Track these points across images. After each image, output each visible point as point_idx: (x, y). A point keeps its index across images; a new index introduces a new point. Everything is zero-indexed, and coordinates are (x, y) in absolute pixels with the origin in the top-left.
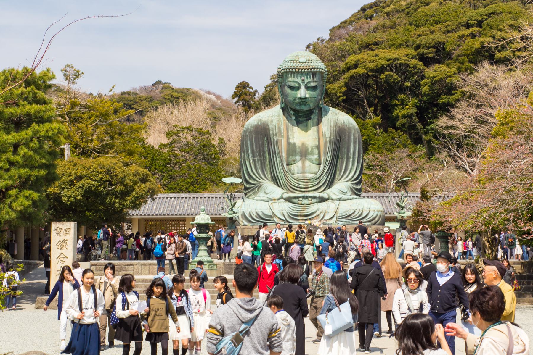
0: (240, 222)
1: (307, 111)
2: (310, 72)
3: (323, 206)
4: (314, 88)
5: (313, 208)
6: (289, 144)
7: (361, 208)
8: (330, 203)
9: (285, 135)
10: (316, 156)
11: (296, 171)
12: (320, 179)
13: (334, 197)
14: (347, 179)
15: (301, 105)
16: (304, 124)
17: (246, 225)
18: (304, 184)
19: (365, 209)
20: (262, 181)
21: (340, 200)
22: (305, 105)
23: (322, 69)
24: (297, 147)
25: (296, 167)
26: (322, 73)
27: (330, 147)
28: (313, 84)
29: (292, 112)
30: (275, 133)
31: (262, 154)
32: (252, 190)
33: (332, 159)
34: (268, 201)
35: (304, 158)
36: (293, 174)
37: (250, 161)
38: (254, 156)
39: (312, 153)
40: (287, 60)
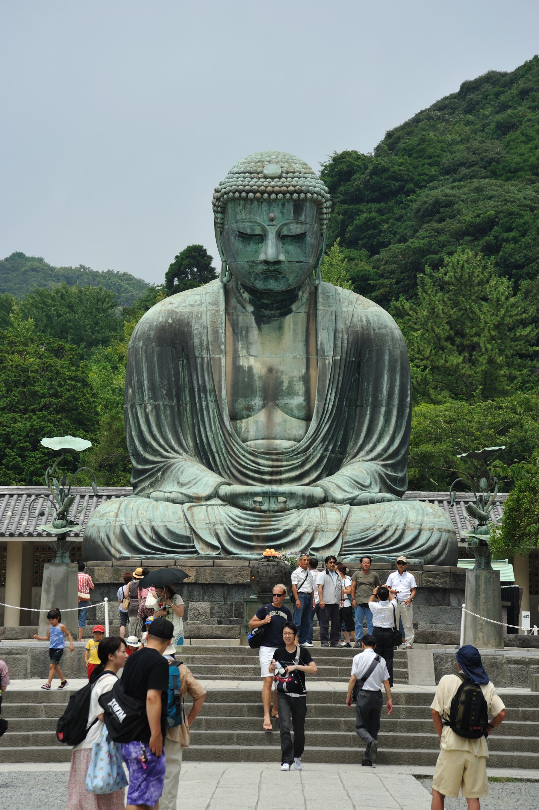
0: (113, 551)
1: (281, 293)
2: (288, 200)
3: (311, 516)
4: (299, 238)
5: (288, 521)
6: (237, 369)
7: (400, 522)
8: (328, 509)
9: (229, 349)
10: (299, 400)
11: (252, 433)
12: (308, 453)
13: (339, 495)
15: (266, 279)
16: (275, 324)
17: (127, 558)
18: (270, 463)
19: (411, 525)
20: (172, 454)
21: (351, 504)
22: (277, 279)
23: (318, 194)
24: (256, 378)
25: (253, 425)
26: (318, 204)
27: (332, 379)
28: (296, 229)
29: (246, 295)
30: (205, 343)
31: (176, 391)
32: (150, 476)
33: (339, 407)
34: (182, 503)
36: (245, 441)
37: (145, 408)
38: (154, 397)
39: (291, 393)
40: (236, 170)
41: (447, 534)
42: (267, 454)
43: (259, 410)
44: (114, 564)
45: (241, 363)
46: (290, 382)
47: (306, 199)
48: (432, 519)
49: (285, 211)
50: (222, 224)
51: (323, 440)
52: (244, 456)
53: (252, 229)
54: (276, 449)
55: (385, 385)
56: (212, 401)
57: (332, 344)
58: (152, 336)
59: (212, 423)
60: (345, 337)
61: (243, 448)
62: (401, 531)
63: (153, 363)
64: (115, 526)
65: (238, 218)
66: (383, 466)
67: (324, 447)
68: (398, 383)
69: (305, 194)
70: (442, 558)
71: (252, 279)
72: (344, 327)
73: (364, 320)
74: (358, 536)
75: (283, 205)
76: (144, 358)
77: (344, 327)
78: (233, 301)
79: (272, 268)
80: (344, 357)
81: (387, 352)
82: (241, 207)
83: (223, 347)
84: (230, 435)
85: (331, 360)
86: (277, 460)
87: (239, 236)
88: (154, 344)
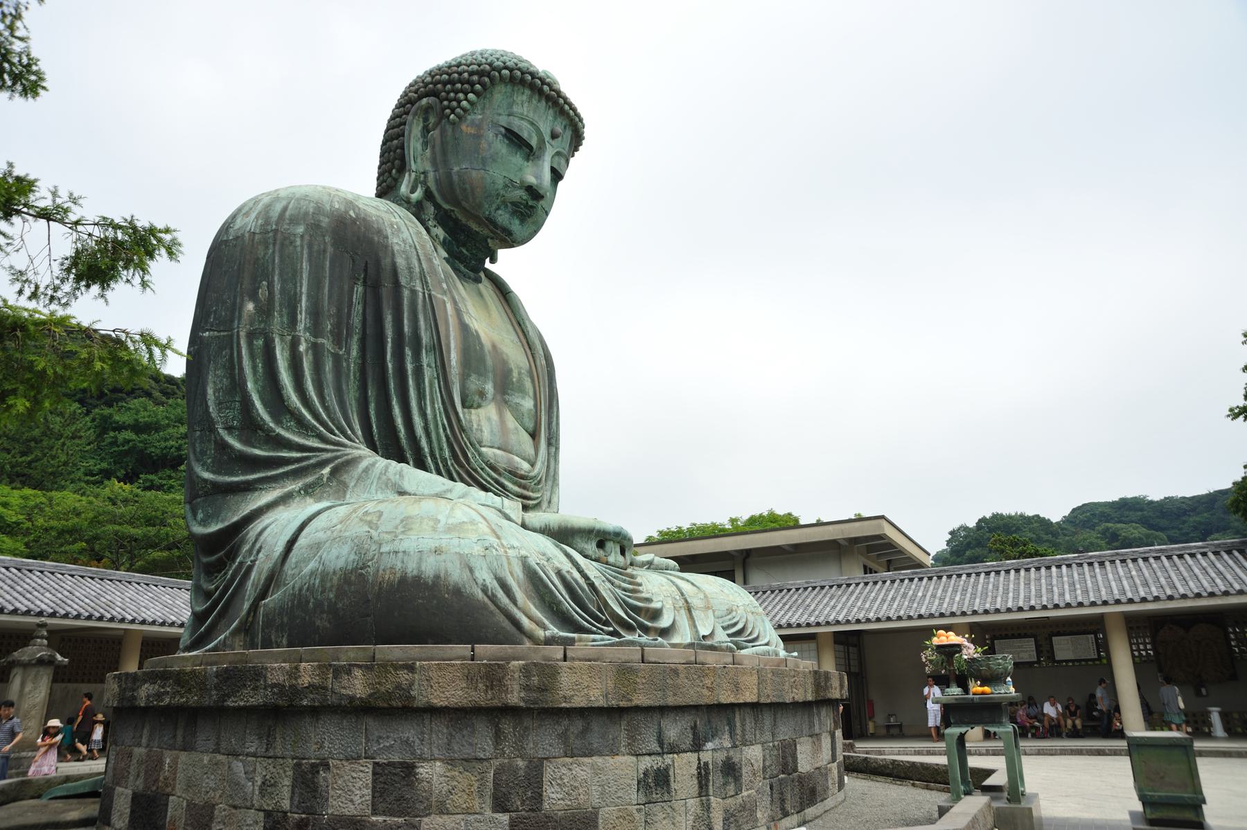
10: (528, 404)
11: (486, 435)
15: (514, 213)
22: (522, 221)
30: (417, 270)
32: (296, 474)
35: (498, 397)
38: (316, 329)
39: (521, 390)
42: (510, 472)
44: (569, 654)
46: (520, 373)
50: (465, 110)
53: (530, 135)
56: (429, 365)
58: (323, 225)
59: (428, 402)
61: (480, 454)
63: (323, 268)
64: (508, 558)
65: (515, 109)
71: (494, 206)
76: (305, 256)
79: (530, 203)
82: (525, 98)
83: (445, 286)
84: (462, 429)
87: (505, 136)
88: (327, 239)
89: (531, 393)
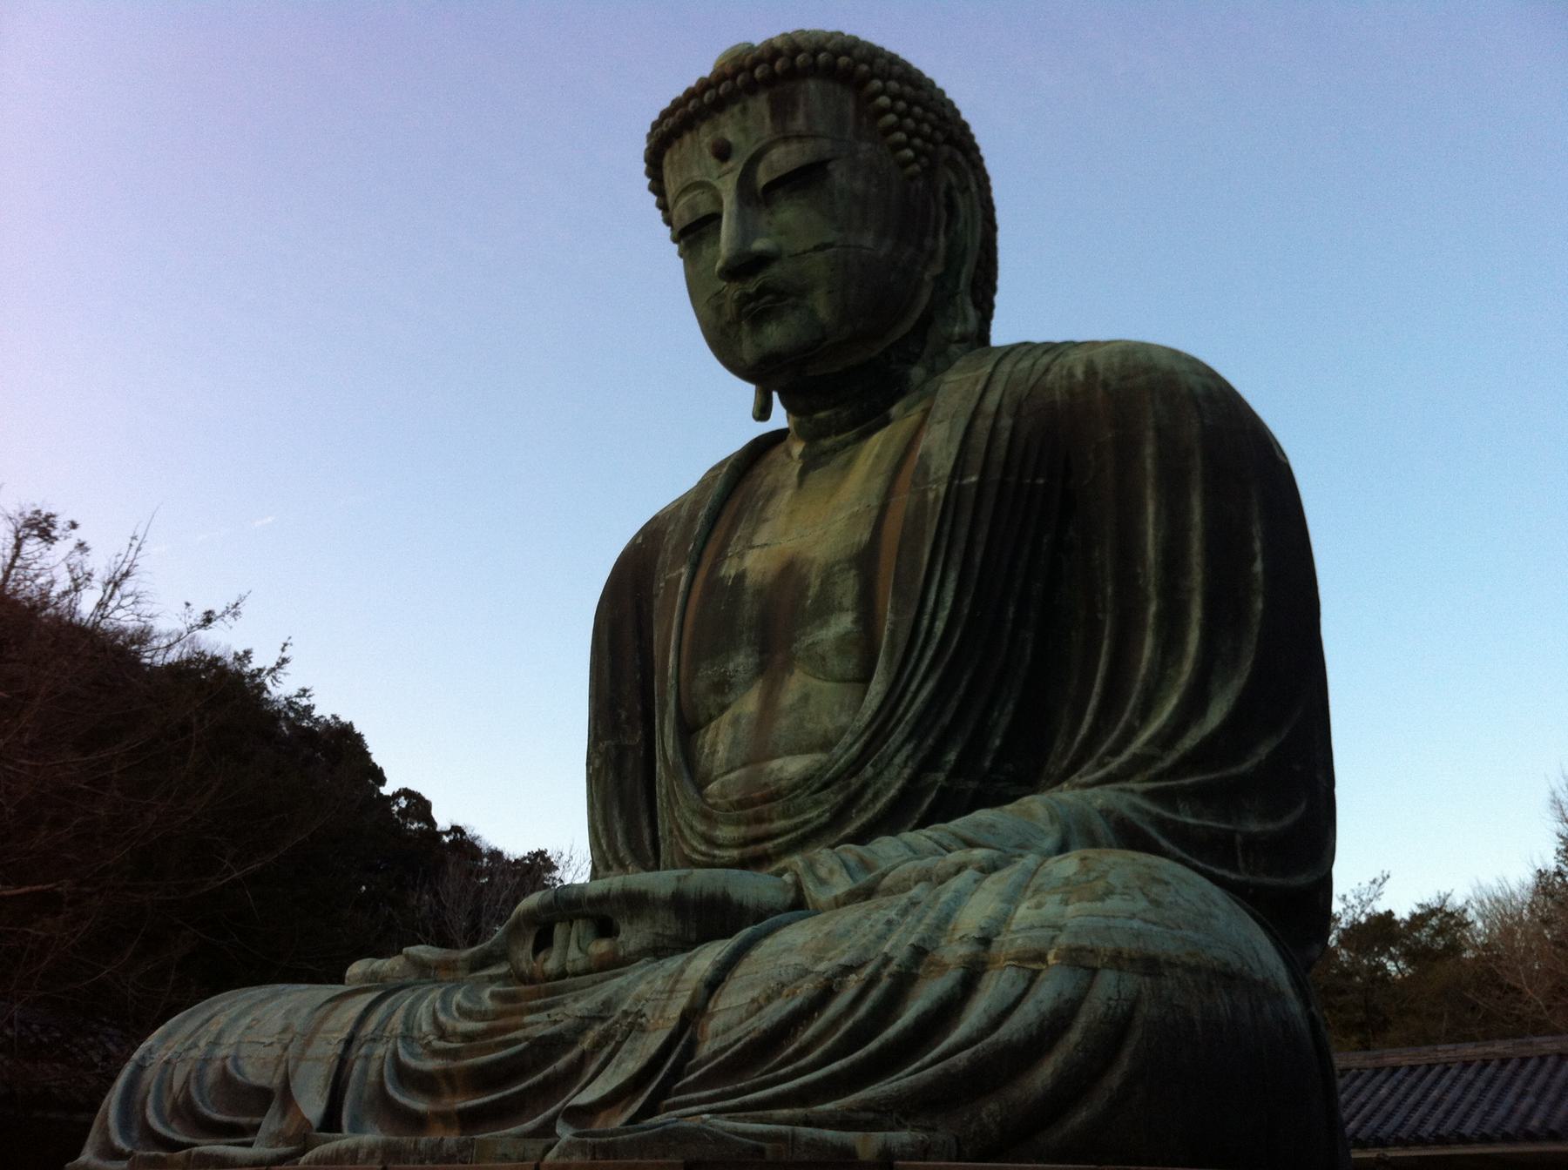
4: (803, 180)
7: (898, 945)
10: (843, 623)
12: (855, 783)
14: (1114, 764)
16: (841, 459)
24: (748, 597)
39: (825, 609)
41: (1132, 982)
43: (748, 685)
45: (723, 572)
47: (793, 73)
48: (1052, 907)
49: (750, 123)
51: (917, 731)
52: (692, 828)
54: (766, 785)
55: (1151, 531)
57: (954, 449)
60: (1006, 422)
62: (885, 982)
66: (1150, 795)
67: (920, 755)
68: (1197, 517)
69: (793, 59)
70: (1081, 1116)
72: (1006, 400)
73: (1079, 372)
74: (733, 1036)
75: (744, 110)
77: (1006, 400)
78: (777, 453)
79: (751, 287)
80: (995, 475)
81: (1150, 434)
85: (943, 489)
86: (759, 820)
89: (848, 601)
